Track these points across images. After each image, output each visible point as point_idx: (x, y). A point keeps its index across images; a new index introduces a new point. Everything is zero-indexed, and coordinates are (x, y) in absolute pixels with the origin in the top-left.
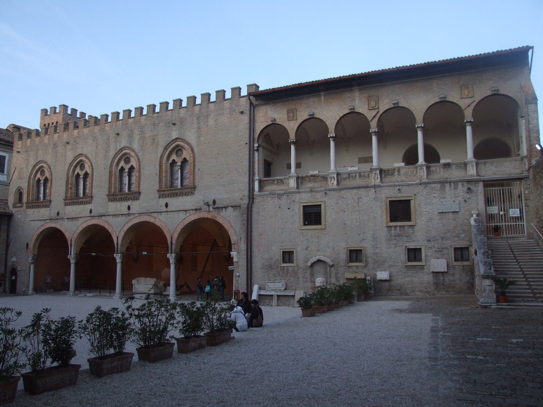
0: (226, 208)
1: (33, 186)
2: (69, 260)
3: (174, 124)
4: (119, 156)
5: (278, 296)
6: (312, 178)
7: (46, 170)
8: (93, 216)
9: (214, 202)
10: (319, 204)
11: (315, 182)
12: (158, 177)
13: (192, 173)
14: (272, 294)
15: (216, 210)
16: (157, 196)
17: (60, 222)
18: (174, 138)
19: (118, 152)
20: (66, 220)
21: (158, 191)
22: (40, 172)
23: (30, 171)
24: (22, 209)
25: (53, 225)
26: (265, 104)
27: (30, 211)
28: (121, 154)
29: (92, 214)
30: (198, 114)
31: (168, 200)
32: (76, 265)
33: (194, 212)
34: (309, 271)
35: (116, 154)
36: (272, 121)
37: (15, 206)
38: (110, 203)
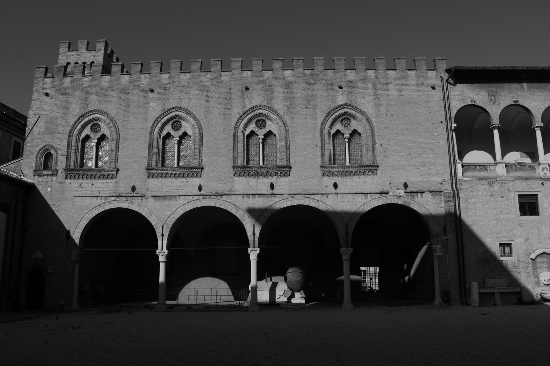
0: (422, 192)
1: (77, 146)
2: (157, 257)
3: (341, 88)
5: (500, 293)
6: (519, 166)
7: (102, 125)
8: (205, 195)
9: (406, 186)
10: (536, 193)
11: (522, 171)
12: (318, 150)
13: (371, 149)
14: (493, 291)
15: (409, 194)
16: (320, 172)
17: (137, 201)
18: (340, 103)
19: (247, 111)
20: (151, 200)
21: (321, 167)
22: (90, 126)
23: (72, 123)
24: (54, 178)
25: (123, 204)
27: (73, 184)
29: (203, 192)
30: (372, 79)
31: (336, 179)
33: (378, 195)
34: (531, 265)
35: (244, 114)
36: (472, 101)
37: (37, 173)
38: (237, 178)
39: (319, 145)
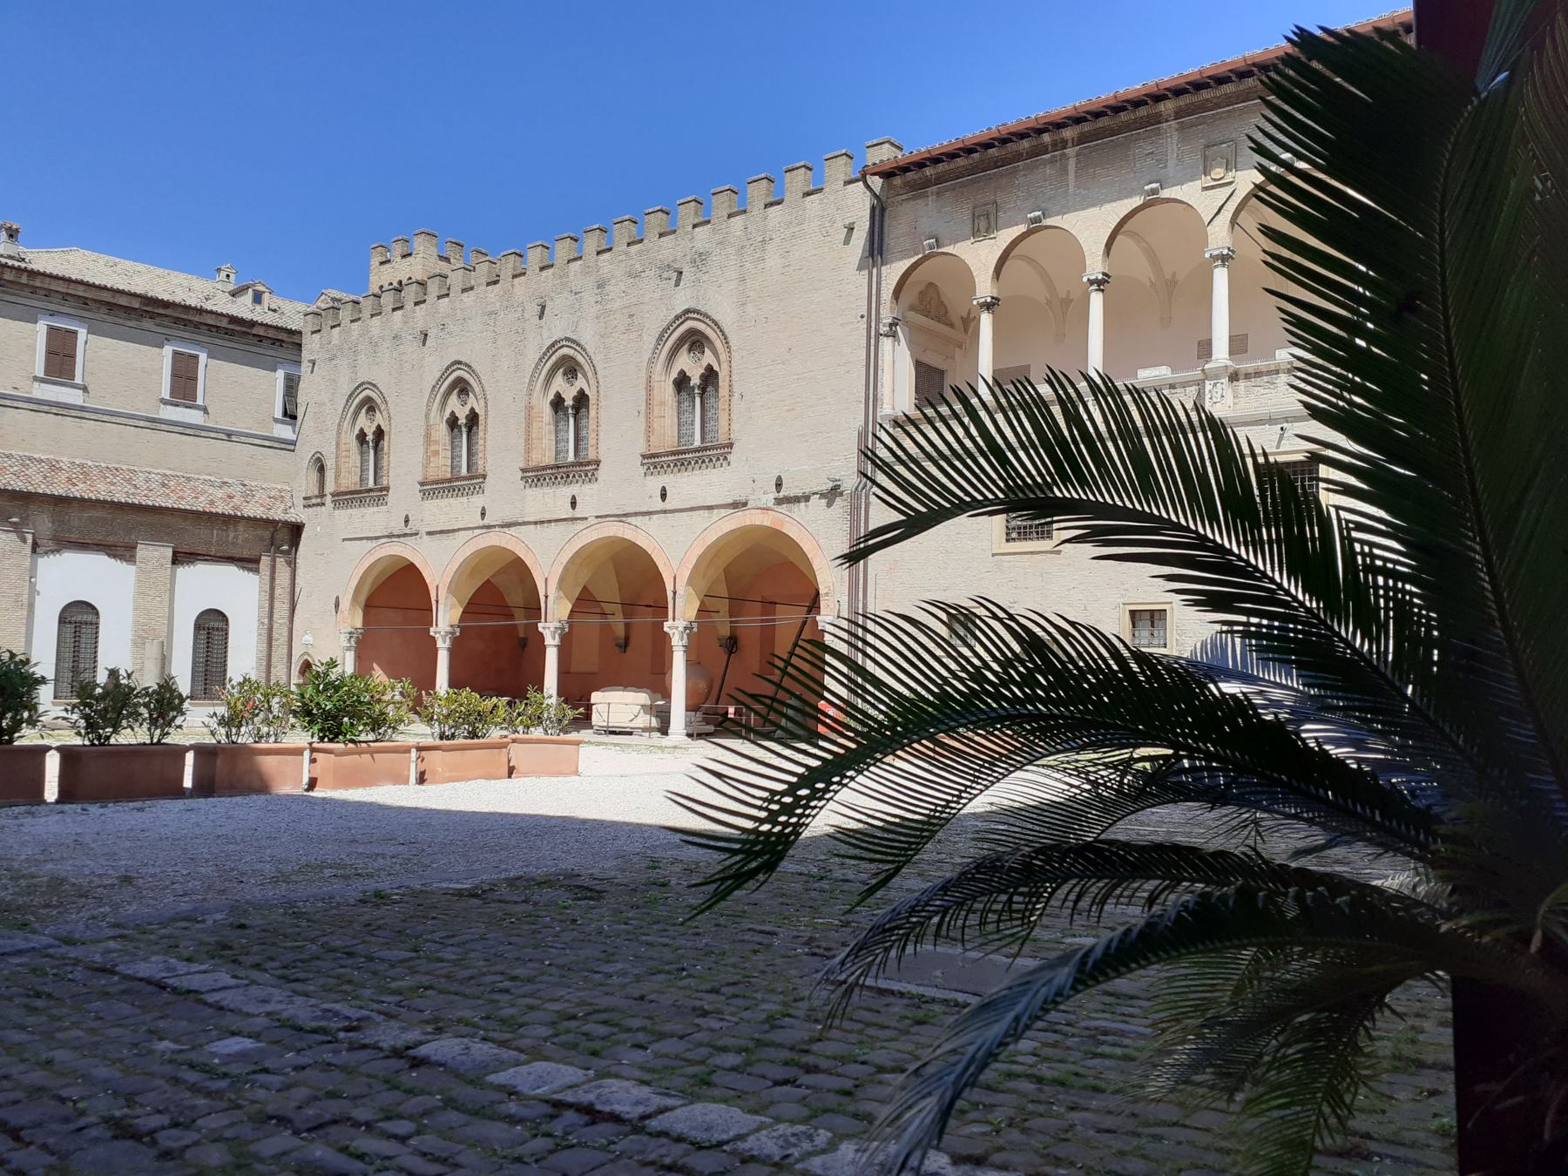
0: (807, 498)
4: (548, 365)
8: (489, 527)
9: (779, 485)
12: (642, 419)
26: (914, 198)
27: (343, 515)
28: (554, 358)
29: (486, 521)
32: (453, 653)
38: (529, 491)
39: (643, 409)
